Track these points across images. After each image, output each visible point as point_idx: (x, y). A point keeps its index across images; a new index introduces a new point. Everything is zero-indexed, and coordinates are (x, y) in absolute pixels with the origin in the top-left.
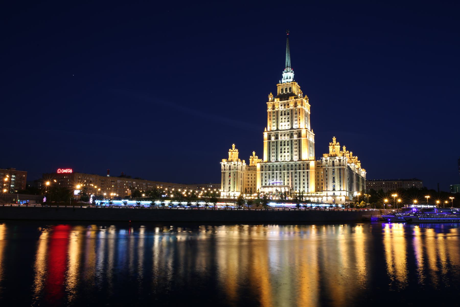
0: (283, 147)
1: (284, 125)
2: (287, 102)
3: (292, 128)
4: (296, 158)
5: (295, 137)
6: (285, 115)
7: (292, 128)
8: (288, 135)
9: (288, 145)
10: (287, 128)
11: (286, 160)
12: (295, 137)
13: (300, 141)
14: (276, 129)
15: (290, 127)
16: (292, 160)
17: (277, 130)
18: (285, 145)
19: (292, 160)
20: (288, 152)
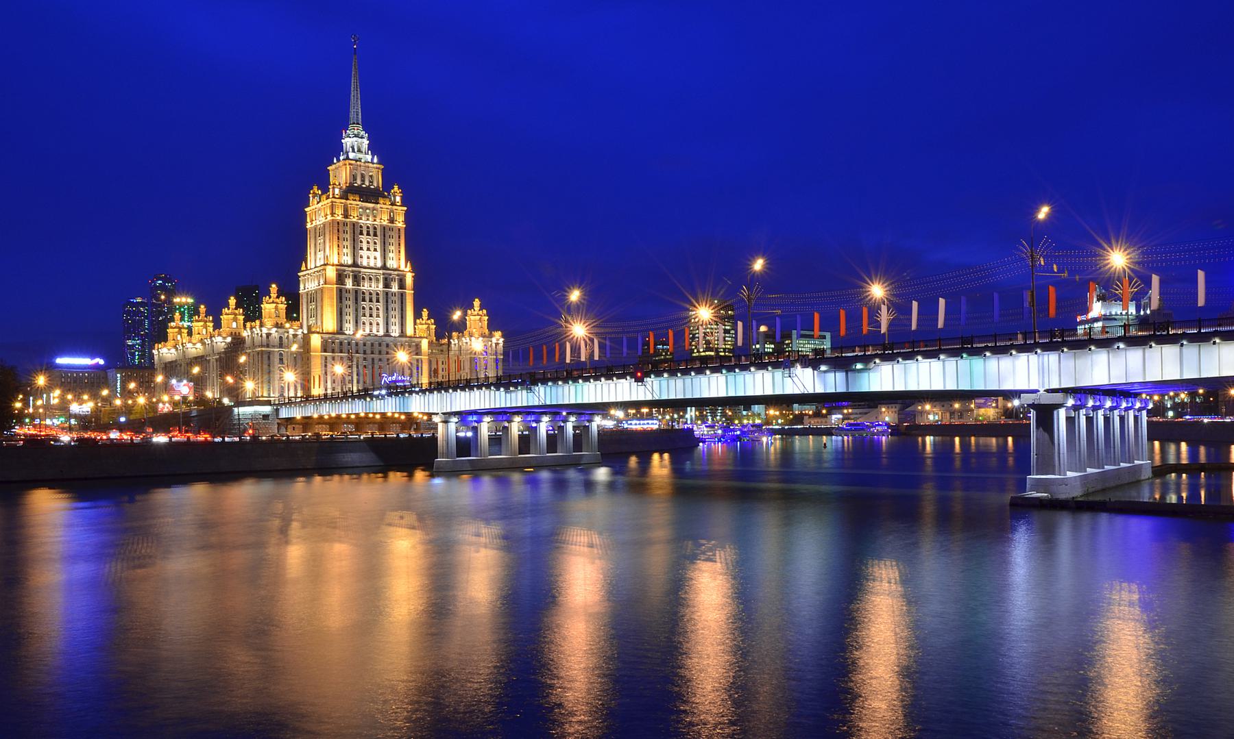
0: (366, 304)
1: (370, 258)
2: (374, 209)
3: (384, 267)
4: (395, 331)
5: (395, 288)
6: (368, 234)
7: (384, 267)
8: (378, 280)
9: (378, 301)
10: (372, 265)
11: (374, 331)
12: (395, 288)
13: (402, 296)
14: (350, 262)
15: (379, 264)
16: (387, 334)
17: (355, 265)
18: (371, 300)
19: (387, 334)
20: (378, 316)
